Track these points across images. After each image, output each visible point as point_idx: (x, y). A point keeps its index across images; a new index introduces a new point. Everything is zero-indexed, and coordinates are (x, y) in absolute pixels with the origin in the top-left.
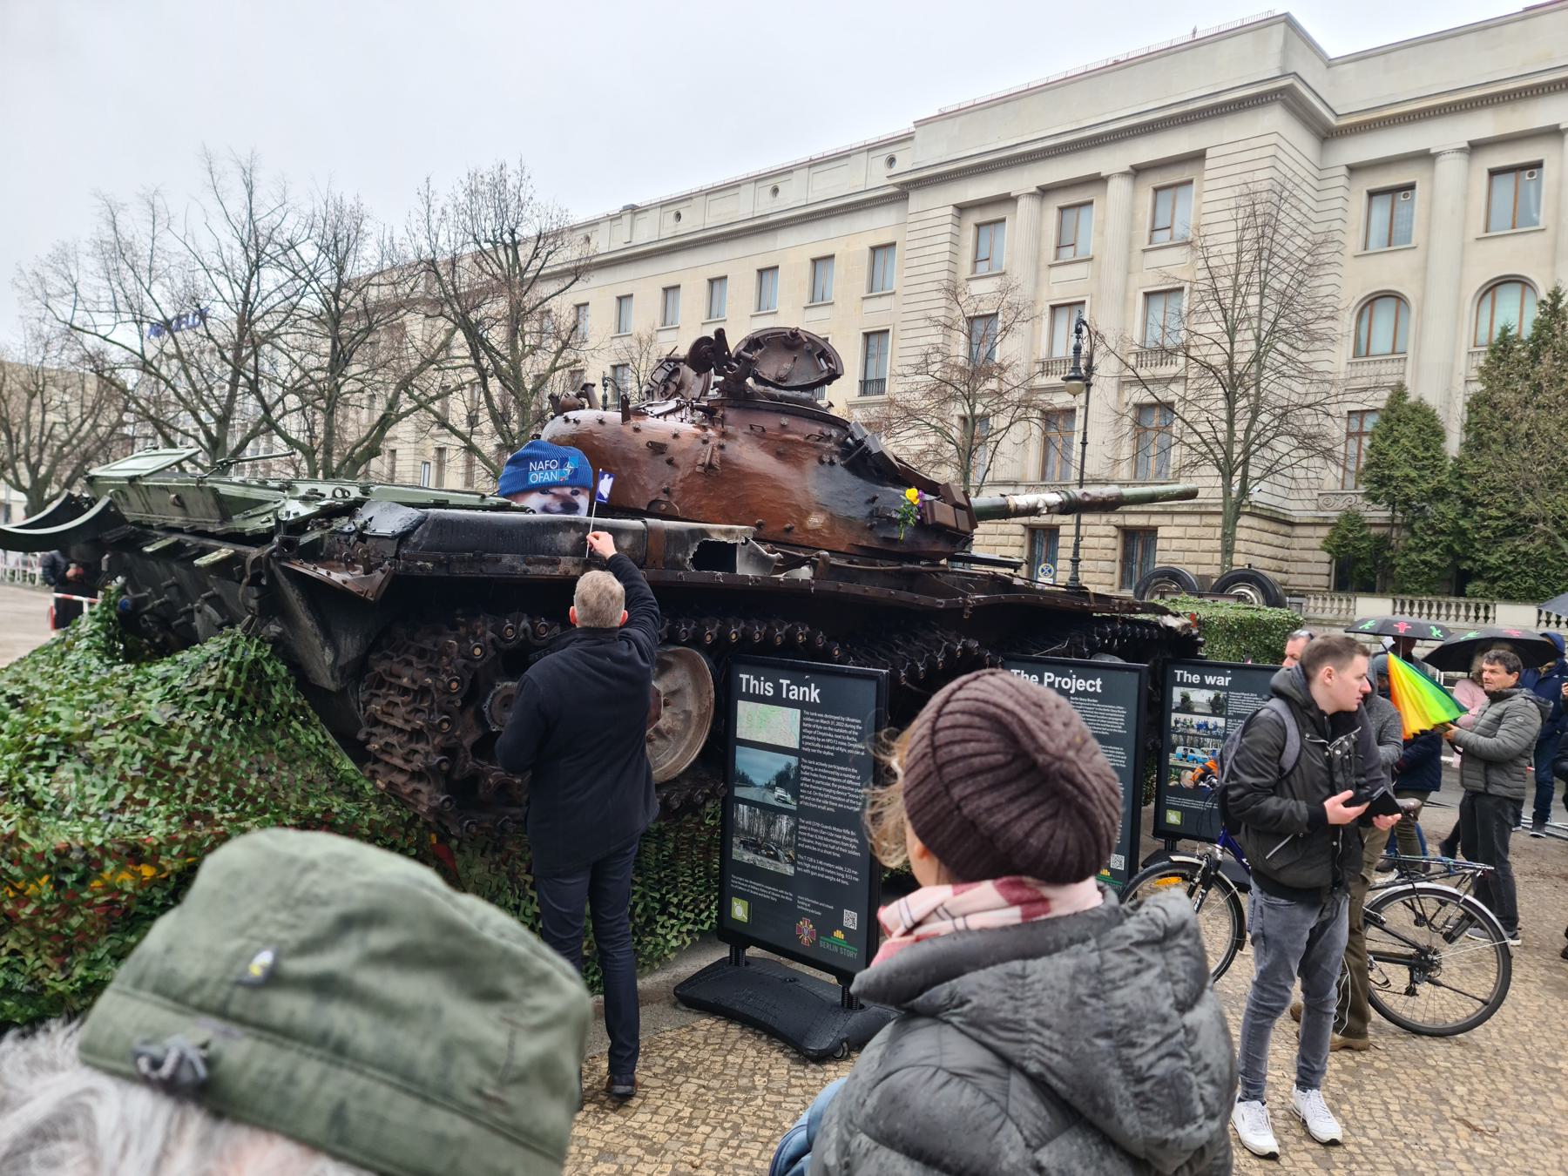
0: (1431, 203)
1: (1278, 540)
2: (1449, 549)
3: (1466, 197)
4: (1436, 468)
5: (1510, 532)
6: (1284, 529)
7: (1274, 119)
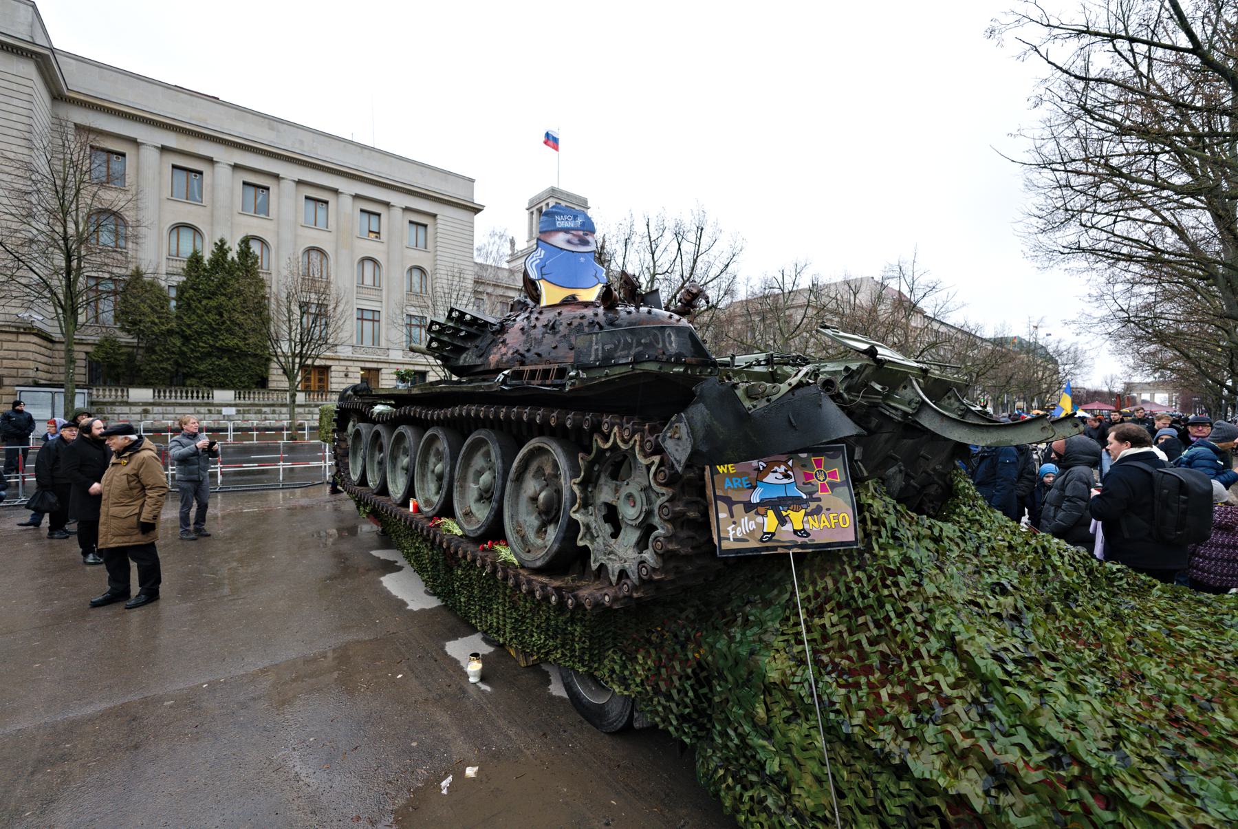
0: (138, 169)
1: (47, 352)
2: (176, 363)
3: (160, 173)
4: (168, 320)
5: (209, 354)
6: (50, 345)
7: (28, 69)
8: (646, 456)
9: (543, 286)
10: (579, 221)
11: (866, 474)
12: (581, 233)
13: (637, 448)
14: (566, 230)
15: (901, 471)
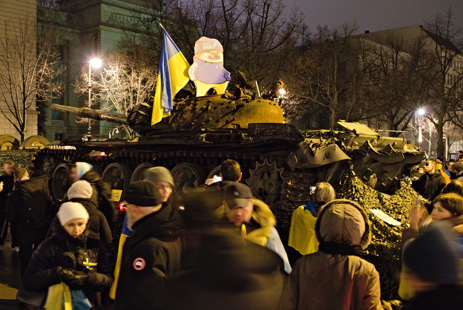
8: (278, 167)
9: (197, 84)
10: (215, 45)
11: (354, 174)
12: (216, 52)
13: (275, 166)
14: (208, 51)
15: (374, 177)
